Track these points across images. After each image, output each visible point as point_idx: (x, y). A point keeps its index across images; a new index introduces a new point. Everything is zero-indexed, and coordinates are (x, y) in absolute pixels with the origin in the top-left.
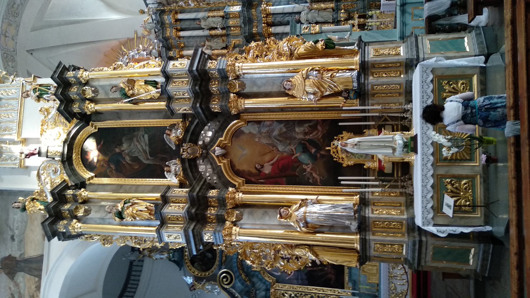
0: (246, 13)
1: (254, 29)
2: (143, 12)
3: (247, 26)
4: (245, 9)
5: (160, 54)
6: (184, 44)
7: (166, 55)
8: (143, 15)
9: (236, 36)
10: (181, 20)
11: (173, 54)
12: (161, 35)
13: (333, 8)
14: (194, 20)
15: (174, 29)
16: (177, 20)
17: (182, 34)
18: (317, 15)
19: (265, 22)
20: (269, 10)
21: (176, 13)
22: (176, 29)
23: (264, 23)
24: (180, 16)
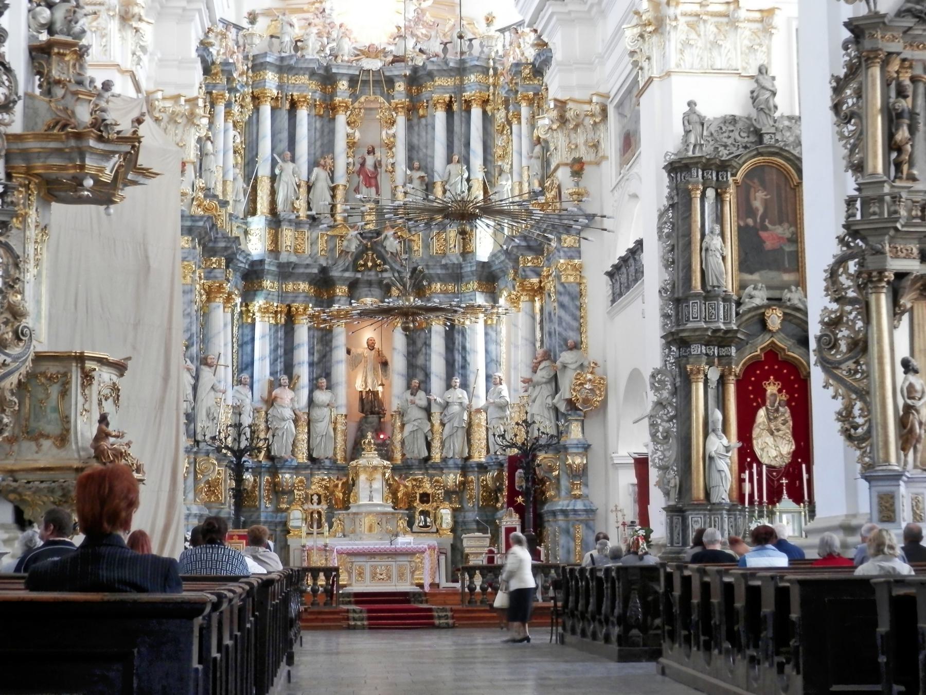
0: (469, 269)
2: (489, 21)
3: (444, 272)
4: (474, 268)
5: (398, 61)
6: (423, 116)
7: (396, 76)
8: (484, 23)
9: (427, 246)
10: (468, 111)
11: (399, 92)
12: (435, 68)
13: (469, 457)
14: (467, 144)
15: (451, 97)
16: (468, 103)
17: (440, 116)
18: (456, 425)
21: (485, 102)
22: (451, 101)
24: (476, 112)
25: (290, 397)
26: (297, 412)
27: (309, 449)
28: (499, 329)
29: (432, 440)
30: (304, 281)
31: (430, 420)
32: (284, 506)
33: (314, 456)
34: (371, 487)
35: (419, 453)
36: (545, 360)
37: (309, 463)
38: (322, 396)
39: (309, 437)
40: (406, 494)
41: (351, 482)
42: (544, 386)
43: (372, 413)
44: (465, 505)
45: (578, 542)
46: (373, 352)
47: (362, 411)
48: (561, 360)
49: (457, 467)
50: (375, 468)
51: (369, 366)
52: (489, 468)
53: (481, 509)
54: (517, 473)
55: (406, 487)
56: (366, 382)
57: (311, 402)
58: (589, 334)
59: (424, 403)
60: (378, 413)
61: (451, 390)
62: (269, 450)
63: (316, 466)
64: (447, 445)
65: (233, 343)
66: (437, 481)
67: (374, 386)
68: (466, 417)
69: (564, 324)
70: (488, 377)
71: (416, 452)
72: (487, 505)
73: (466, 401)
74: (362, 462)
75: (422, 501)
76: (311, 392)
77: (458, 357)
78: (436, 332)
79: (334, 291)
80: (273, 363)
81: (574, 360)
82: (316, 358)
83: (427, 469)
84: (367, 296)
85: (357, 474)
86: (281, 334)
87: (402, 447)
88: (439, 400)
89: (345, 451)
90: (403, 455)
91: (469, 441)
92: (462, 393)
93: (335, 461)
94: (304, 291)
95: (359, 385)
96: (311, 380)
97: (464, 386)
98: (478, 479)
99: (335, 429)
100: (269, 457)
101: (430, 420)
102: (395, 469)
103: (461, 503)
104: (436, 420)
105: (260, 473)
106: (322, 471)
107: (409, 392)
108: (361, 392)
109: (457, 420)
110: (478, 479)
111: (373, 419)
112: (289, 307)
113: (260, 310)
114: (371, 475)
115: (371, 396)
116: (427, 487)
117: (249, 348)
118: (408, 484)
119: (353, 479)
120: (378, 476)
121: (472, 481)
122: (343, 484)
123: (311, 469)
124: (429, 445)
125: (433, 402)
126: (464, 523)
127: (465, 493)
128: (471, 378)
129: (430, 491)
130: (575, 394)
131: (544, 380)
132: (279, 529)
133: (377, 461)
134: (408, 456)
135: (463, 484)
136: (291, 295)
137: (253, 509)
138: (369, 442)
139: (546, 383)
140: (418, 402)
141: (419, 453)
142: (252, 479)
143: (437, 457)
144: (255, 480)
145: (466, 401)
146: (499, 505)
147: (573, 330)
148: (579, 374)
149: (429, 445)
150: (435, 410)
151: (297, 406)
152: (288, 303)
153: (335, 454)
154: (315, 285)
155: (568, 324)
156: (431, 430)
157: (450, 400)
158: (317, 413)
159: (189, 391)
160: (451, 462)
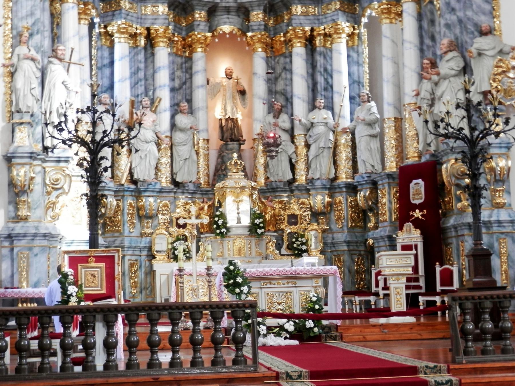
1: (299, 7)
13: (336, 178)
18: (322, 145)
19: (315, 33)
20: (339, 40)
23: (312, 30)
25: (152, 119)
26: (159, 135)
27: (172, 174)
28: (360, 50)
29: (296, 162)
30: (163, 3)
31: (293, 142)
32: (148, 231)
33: (178, 180)
34: (238, 209)
35: (283, 175)
36: (451, 51)
37: (172, 187)
38: (182, 120)
39: (172, 161)
40: (274, 216)
41: (217, 204)
42: (452, 79)
43: (232, 140)
44: (333, 227)
45: (504, 258)
46: (231, 81)
47: (222, 140)
48: (475, 46)
49: (324, 188)
50: (243, 188)
51: (228, 95)
52: (359, 188)
53: (351, 229)
54: (412, 185)
55: (274, 209)
56: (225, 110)
57: (173, 126)
58: (501, 19)
59: (287, 125)
60: (238, 140)
61: (316, 110)
62: (131, 173)
63: (180, 190)
64: (313, 166)
65: (91, 66)
66: (303, 203)
67: (233, 113)
68: (331, 137)
69: (474, 7)
70: (352, 98)
71: (280, 174)
72: (356, 226)
73: (331, 121)
74: (229, 183)
75: (290, 223)
76: (173, 117)
77: (320, 79)
78: (298, 54)
79: (193, 16)
80: (134, 86)
81: (492, 46)
82: (177, 84)
83: (292, 191)
84: (225, 23)
85: (224, 196)
86: (141, 57)
87: (266, 171)
88: (304, 121)
89: (208, 175)
90: (267, 178)
91: (335, 163)
92: (327, 114)
93: (199, 186)
94: (163, 13)
95: (218, 113)
96: (172, 106)
97: (330, 107)
98: (347, 200)
99: (197, 153)
100: (134, 182)
101: (293, 142)
102: (261, 192)
103: (328, 224)
104: (300, 141)
105: (123, 196)
106: (187, 195)
107: (271, 115)
108: (221, 120)
109: (323, 140)
110: (347, 200)
111: (233, 145)
112: (148, 29)
113: (119, 31)
114: (237, 197)
115: (230, 124)
116: (295, 209)
117: (107, 71)
118: (277, 206)
119: (219, 201)
120: (245, 198)
121: (340, 202)
122: (209, 206)
123: (175, 193)
124: (293, 167)
125: (297, 122)
126: (333, 244)
127: (332, 214)
128: (336, 99)
129: (297, 213)
130: (495, 85)
131: (453, 72)
132: (145, 253)
133: (244, 182)
134: (272, 179)
135: (330, 204)
136: (151, 17)
137: (116, 234)
138: (236, 163)
139: (455, 76)
140: (281, 124)
141: (283, 175)
142: (115, 203)
143: (301, 178)
144: (118, 204)
145: (331, 121)
146: (371, 225)
147: (484, 14)
148: (501, 60)
149: (293, 167)
150: (299, 132)
151: (158, 129)
152: (147, 25)
153: (199, 179)
154: (174, 10)
155: (479, 7)
156: (295, 152)
157: (315, 121)
158: (179, 137)
159: (36, 84)
160: (318, 183)
